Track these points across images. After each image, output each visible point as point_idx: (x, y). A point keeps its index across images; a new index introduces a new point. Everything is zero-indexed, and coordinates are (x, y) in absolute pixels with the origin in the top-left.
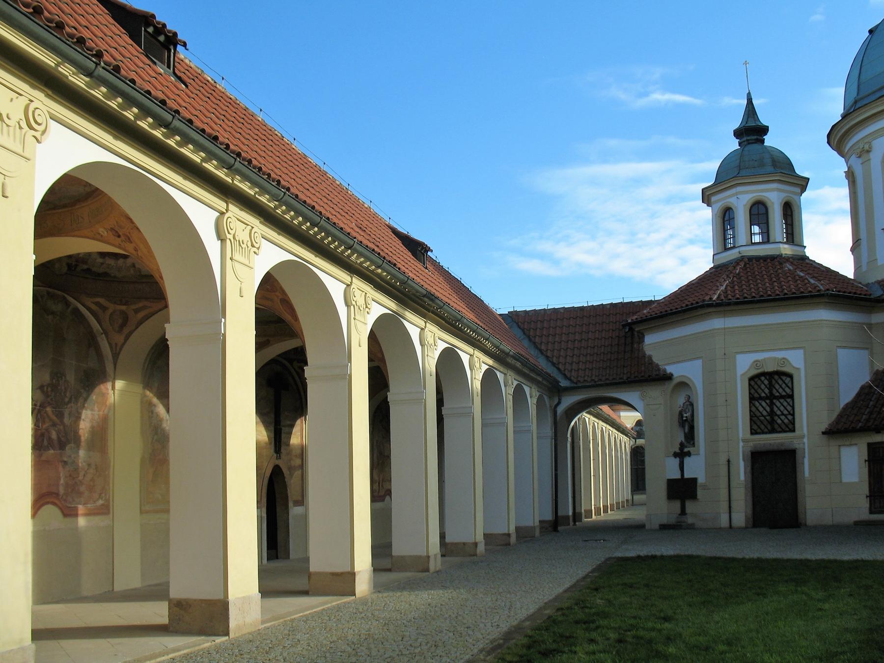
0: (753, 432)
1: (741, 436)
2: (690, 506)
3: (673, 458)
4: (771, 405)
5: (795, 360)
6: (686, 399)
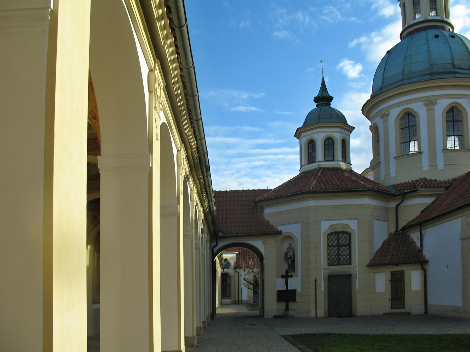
0: (329, 265)
1: (322, 266)
2: (292, 305)
3: (281, 278)
4: (339, 250)
5: (353, 225)
6: (290, 245)
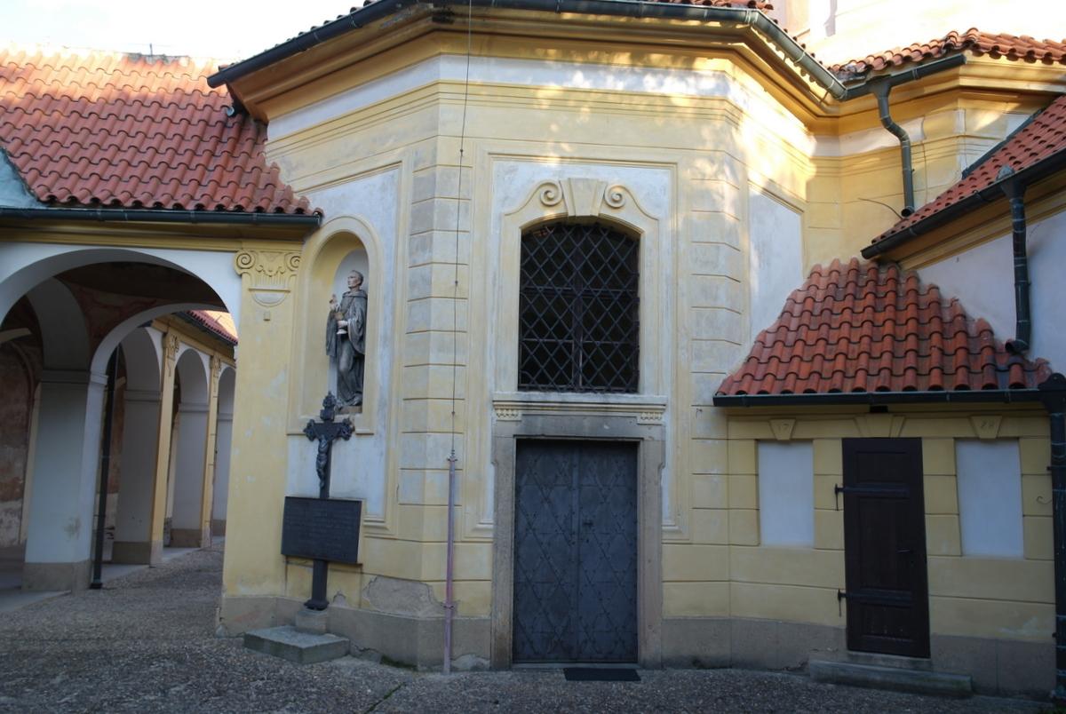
3: (305, 440)
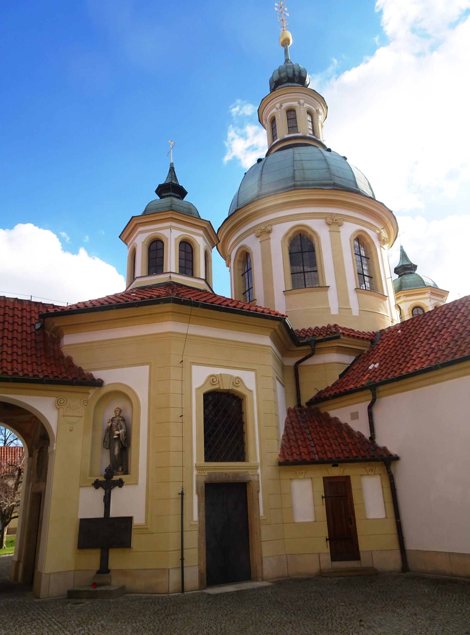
0: (208, 458)
1: (195, 462)
3: (93, 488)
